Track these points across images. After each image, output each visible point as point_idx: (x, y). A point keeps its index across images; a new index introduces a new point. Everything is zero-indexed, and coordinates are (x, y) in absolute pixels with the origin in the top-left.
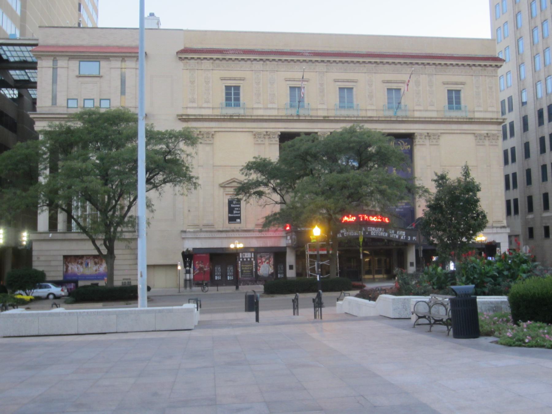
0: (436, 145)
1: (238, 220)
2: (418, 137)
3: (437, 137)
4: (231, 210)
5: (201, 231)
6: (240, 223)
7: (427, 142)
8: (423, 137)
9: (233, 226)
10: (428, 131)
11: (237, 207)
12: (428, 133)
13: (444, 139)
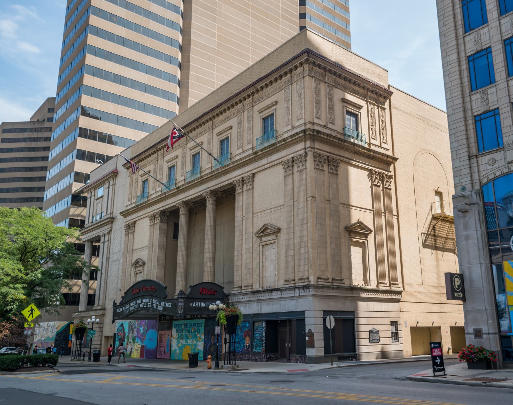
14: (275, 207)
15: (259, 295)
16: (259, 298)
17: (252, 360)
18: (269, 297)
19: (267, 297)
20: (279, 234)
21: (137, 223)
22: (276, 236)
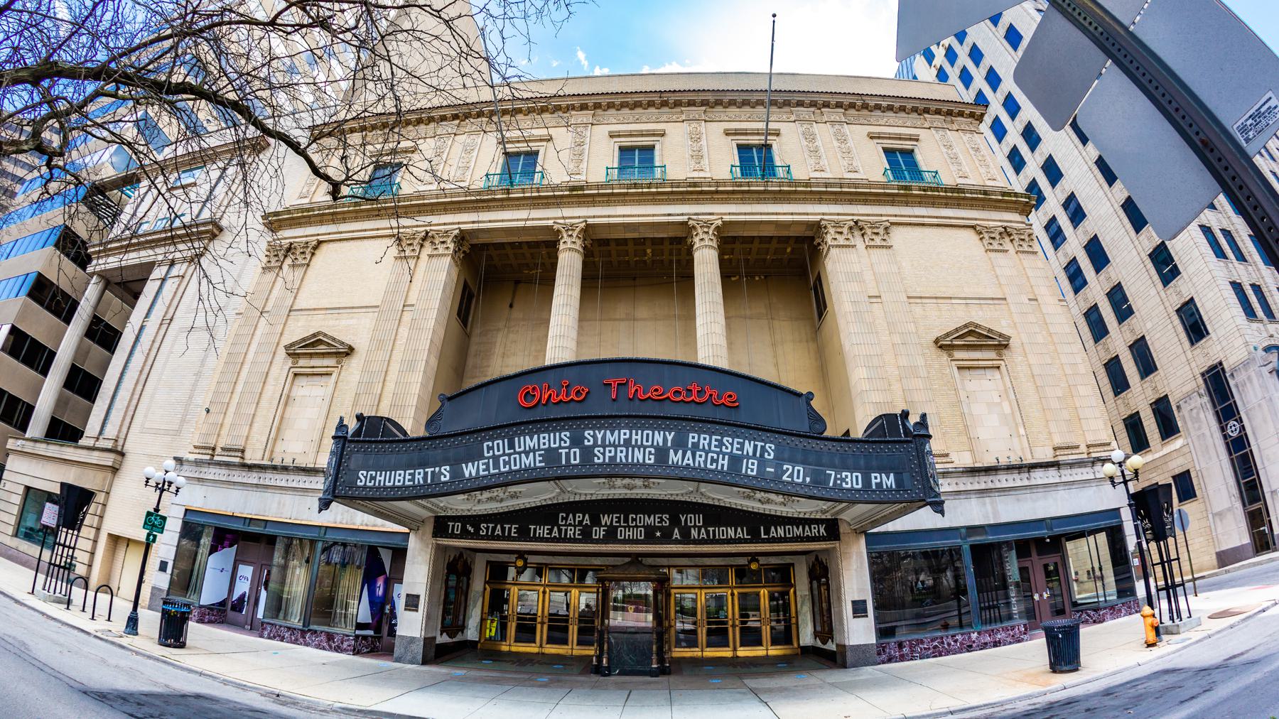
0: (883, 247)
2: (832, 231)
3: (881, 231)
5: (212, 463)
7: (857, 240)
8: (845, 230)
10: (856, 218)
12: (856, 223)
13: (899, 236)
15: (991, 478)
16: (991, 486)
17: (984, 646)
18: (1026, 483)
19: (1019, 483)
20: (1005, 351)
21: (324, 247)
22: (1000, 355)
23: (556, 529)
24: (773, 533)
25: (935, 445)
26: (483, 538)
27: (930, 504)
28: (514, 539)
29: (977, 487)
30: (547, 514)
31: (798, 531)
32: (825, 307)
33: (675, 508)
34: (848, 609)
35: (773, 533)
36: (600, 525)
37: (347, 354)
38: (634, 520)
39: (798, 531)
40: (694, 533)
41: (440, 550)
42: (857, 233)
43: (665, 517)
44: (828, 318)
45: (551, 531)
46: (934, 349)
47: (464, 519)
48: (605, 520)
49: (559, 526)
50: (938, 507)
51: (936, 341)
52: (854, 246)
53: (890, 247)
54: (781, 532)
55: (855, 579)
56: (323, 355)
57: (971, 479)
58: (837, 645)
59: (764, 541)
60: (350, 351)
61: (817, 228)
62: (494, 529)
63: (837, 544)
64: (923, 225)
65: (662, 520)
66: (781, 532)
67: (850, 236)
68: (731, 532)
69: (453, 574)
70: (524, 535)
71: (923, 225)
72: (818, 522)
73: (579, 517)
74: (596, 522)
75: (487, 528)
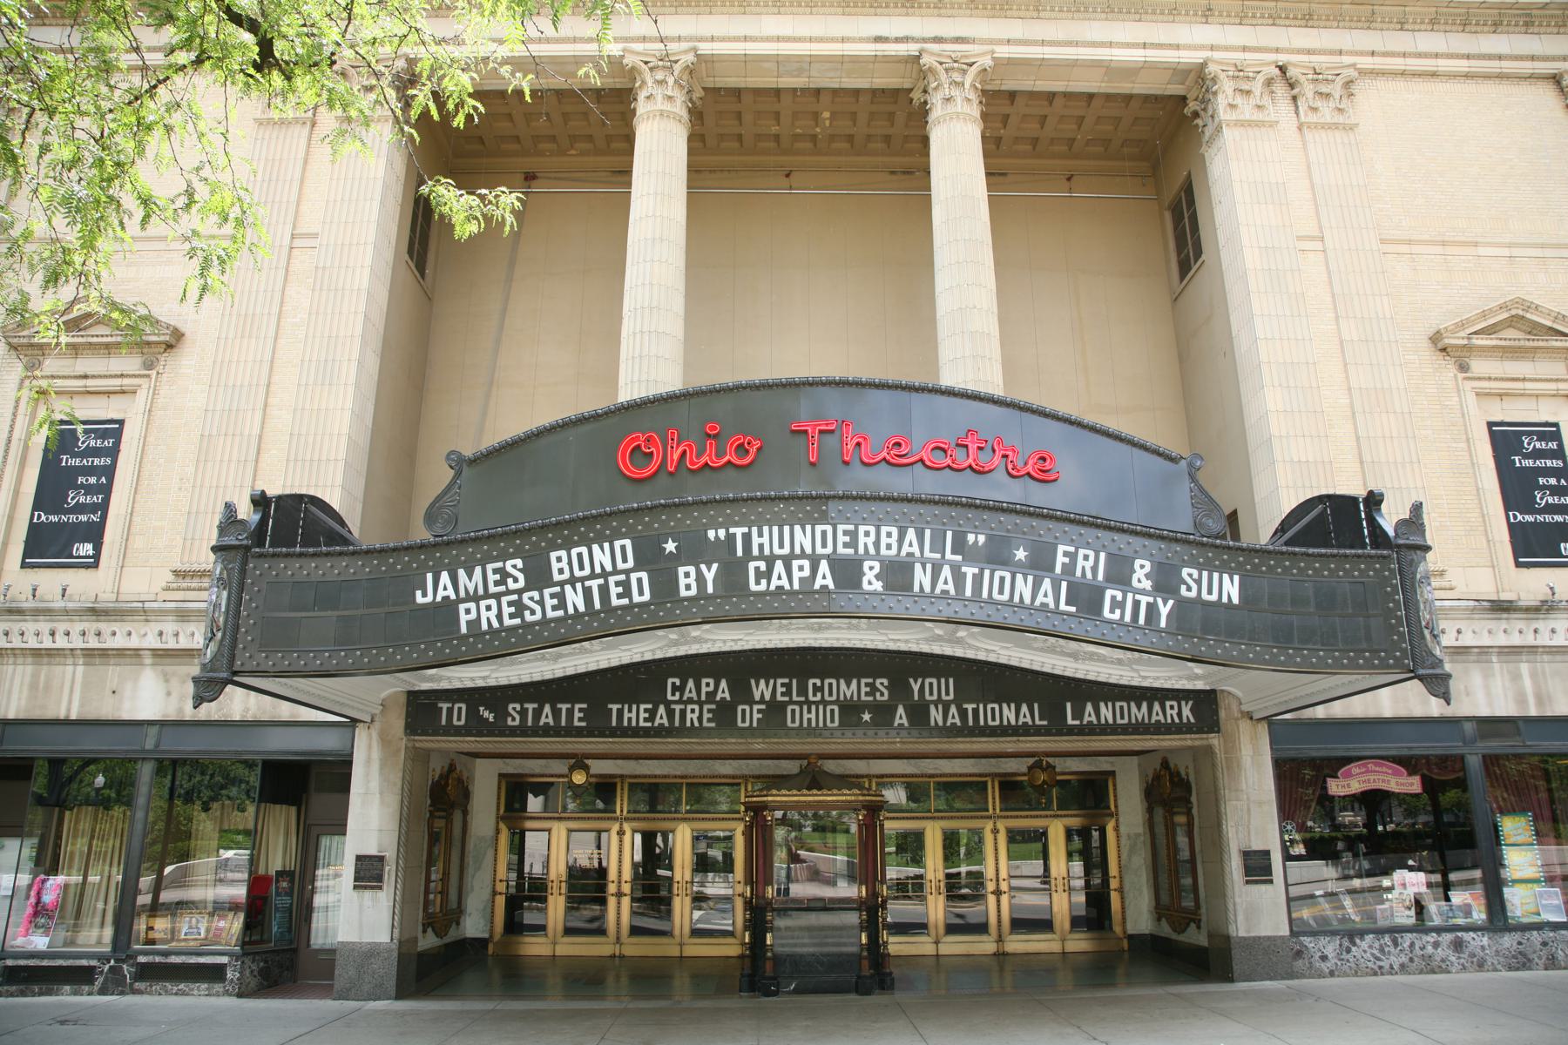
0: (1334, 126)
1: (87, 549)
3: (1336, 89)
4: (54, 484)
6: (94, 563)
8: (1257, 86)
9: (50, 582)
10: (1282, 58)
11: (90, 471)
12: (1282, 69)
13: (1373, 100)
14: (1543, 246)
16: (1529, 640)
23: (662, 710)
24: (1089, 715)
25: (1432, 561)
26: (513, 732)
27: (1421, 678)
28: (579, 732)
29: (1502, 640)
30: (640, 681)
31: (1139, 713)
32: (1198, 252)
33: (901, 667)
34: (1235, 865)
35: (1089, 715)
36: (751, 702)
37: (169, 346)
38: (816, 689)
39: (1139, 713)
40: (936, 715)
41: (418, 758)
42: (1280, 89)
43: (881, 683)
44: (1201, 278)
45: (652, 714)
46: (1426, 344)
47: (473, 696)
48: (761, 689)
49: (668, 704)
50: (1438, 684)
51: (1435, 338)
52: (1273, 124)
53: (1352, 128)
54: (1106, 713)
55: (1252, 811)
56: (109, 349)
57: (1492, 625)
58: (1210, 936)
59: (1072, 731)
60: (174, 341)
61: (1199, 77)
62: (538, 713)
63: (1214, 740)
64: (1434, 75)
65: (873, 689)
66: (1106, 713)
67: (1266, 101)
68: (1009, 714)
69: (437, 804)
70: (598, 725)
71: (1434, 75)
72: (1179, 695)
73: (707, 684)
74: (742, 693)
75: (523, 713)
